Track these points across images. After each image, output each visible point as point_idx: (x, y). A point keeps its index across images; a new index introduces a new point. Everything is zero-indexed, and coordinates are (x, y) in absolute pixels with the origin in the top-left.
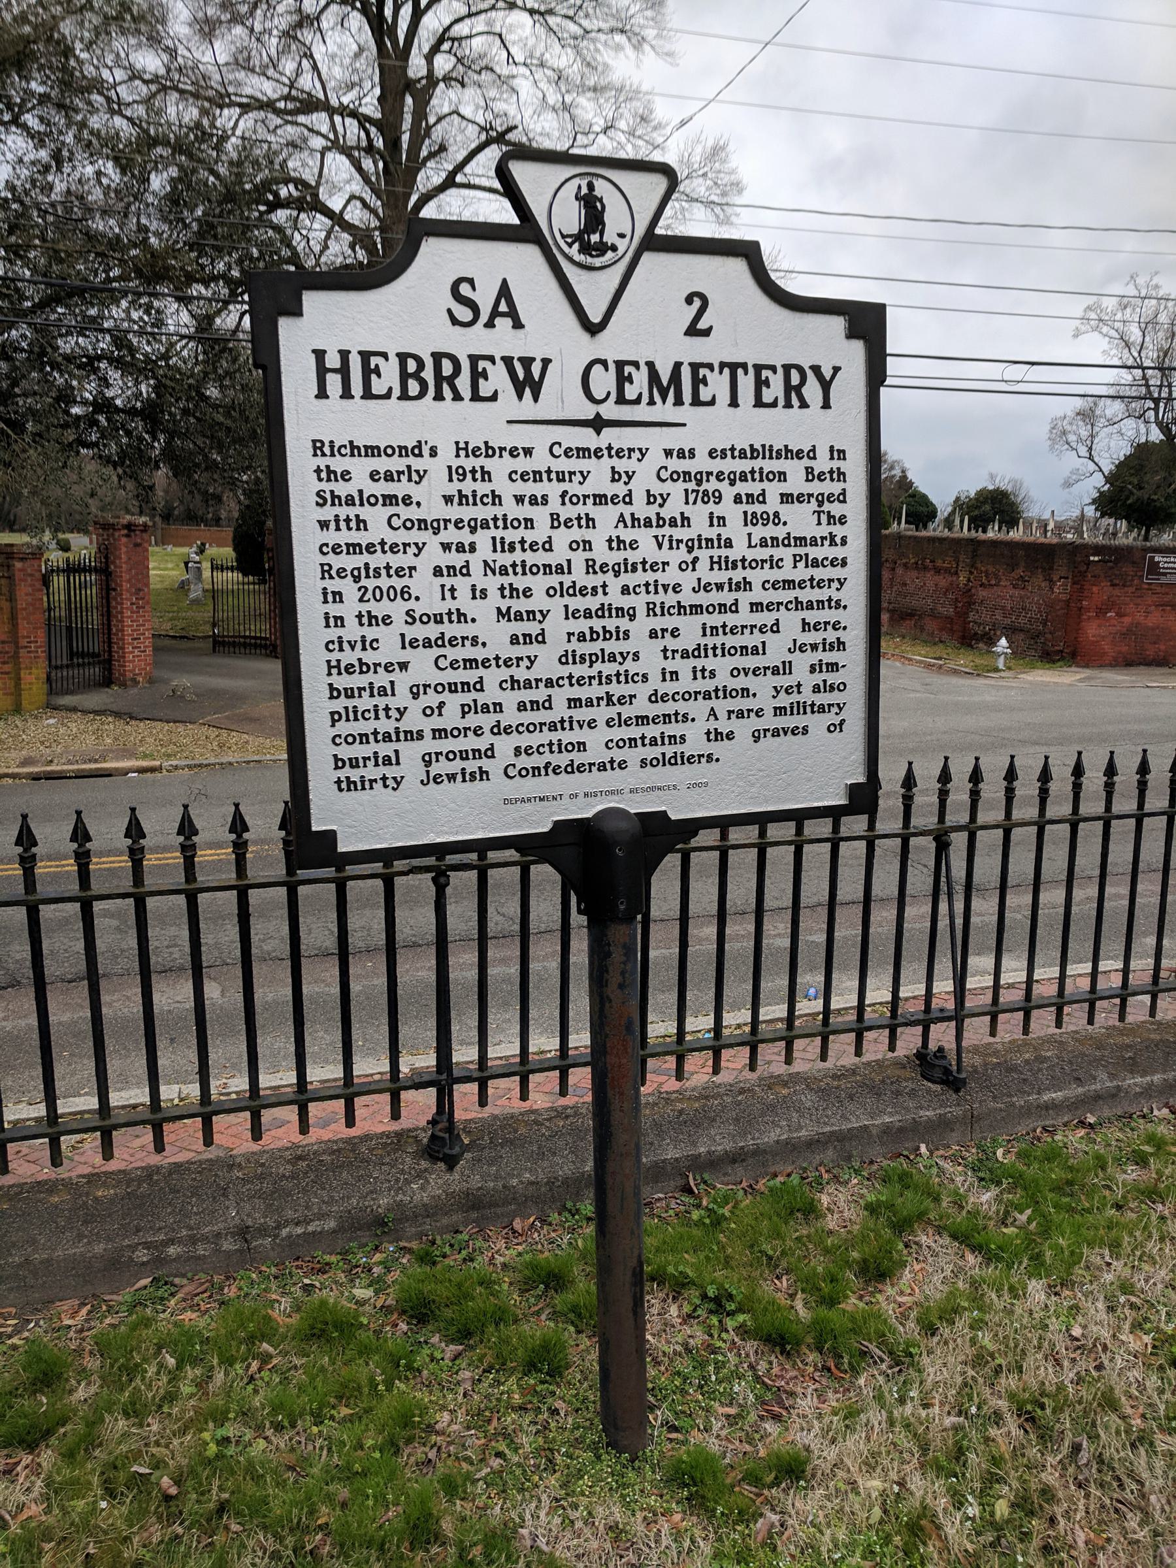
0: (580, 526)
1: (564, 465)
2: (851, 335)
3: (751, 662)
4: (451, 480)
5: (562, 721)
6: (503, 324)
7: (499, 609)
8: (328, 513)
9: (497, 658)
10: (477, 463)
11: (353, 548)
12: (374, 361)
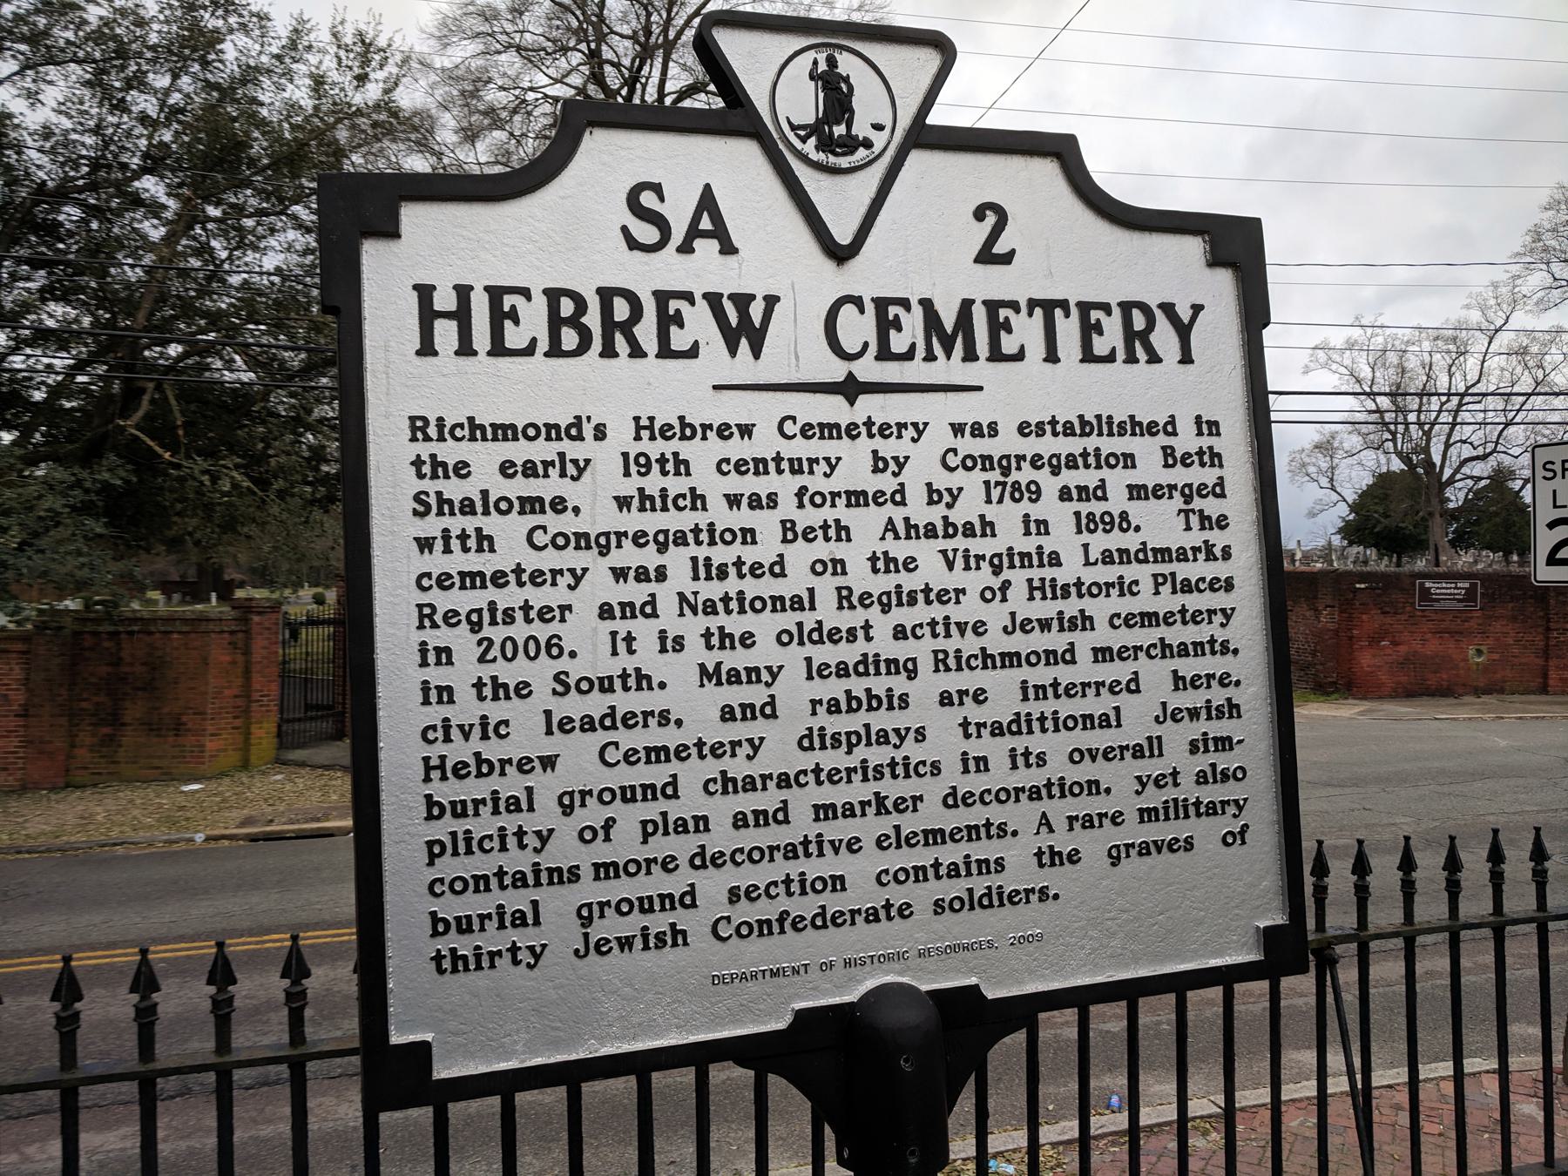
0: (827, 539)
1: (801, 449)
2: (1214, 262)
3: (1099, 739)
4: (627, 474)
5: (806, 842)
6: (707, 248)
7: (702, 666)
8: (432, 526)
9: (700, 744)
10: (668, 447)
11: (472, 580)
12: (508, 301)
